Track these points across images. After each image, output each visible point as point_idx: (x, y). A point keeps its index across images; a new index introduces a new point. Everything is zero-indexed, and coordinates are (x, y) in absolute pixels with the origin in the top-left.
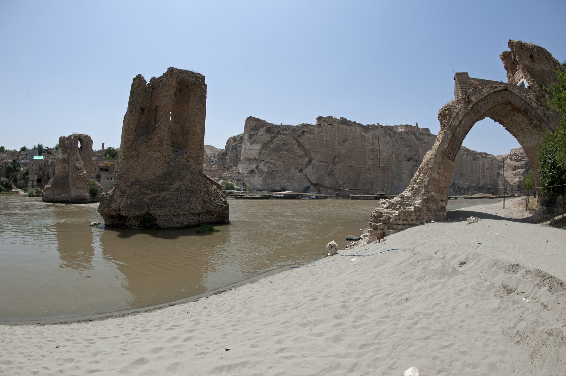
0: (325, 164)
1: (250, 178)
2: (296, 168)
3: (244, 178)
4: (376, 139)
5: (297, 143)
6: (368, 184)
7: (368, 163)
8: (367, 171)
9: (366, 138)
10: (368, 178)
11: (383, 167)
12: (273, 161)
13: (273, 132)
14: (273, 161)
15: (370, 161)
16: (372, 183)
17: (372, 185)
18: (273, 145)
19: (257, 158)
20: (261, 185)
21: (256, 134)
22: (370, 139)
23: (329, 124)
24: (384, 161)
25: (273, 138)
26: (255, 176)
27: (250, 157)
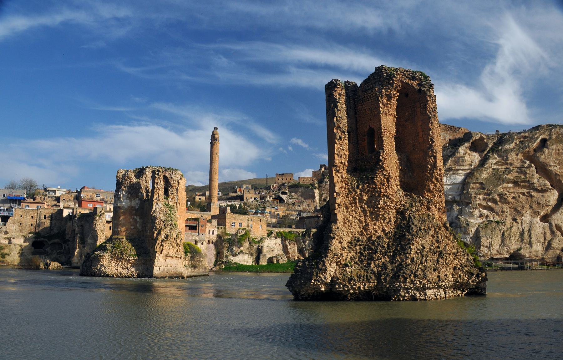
2: (535, 213)
5: (533, 165)
18: (486, 173)
19: (458, 199)
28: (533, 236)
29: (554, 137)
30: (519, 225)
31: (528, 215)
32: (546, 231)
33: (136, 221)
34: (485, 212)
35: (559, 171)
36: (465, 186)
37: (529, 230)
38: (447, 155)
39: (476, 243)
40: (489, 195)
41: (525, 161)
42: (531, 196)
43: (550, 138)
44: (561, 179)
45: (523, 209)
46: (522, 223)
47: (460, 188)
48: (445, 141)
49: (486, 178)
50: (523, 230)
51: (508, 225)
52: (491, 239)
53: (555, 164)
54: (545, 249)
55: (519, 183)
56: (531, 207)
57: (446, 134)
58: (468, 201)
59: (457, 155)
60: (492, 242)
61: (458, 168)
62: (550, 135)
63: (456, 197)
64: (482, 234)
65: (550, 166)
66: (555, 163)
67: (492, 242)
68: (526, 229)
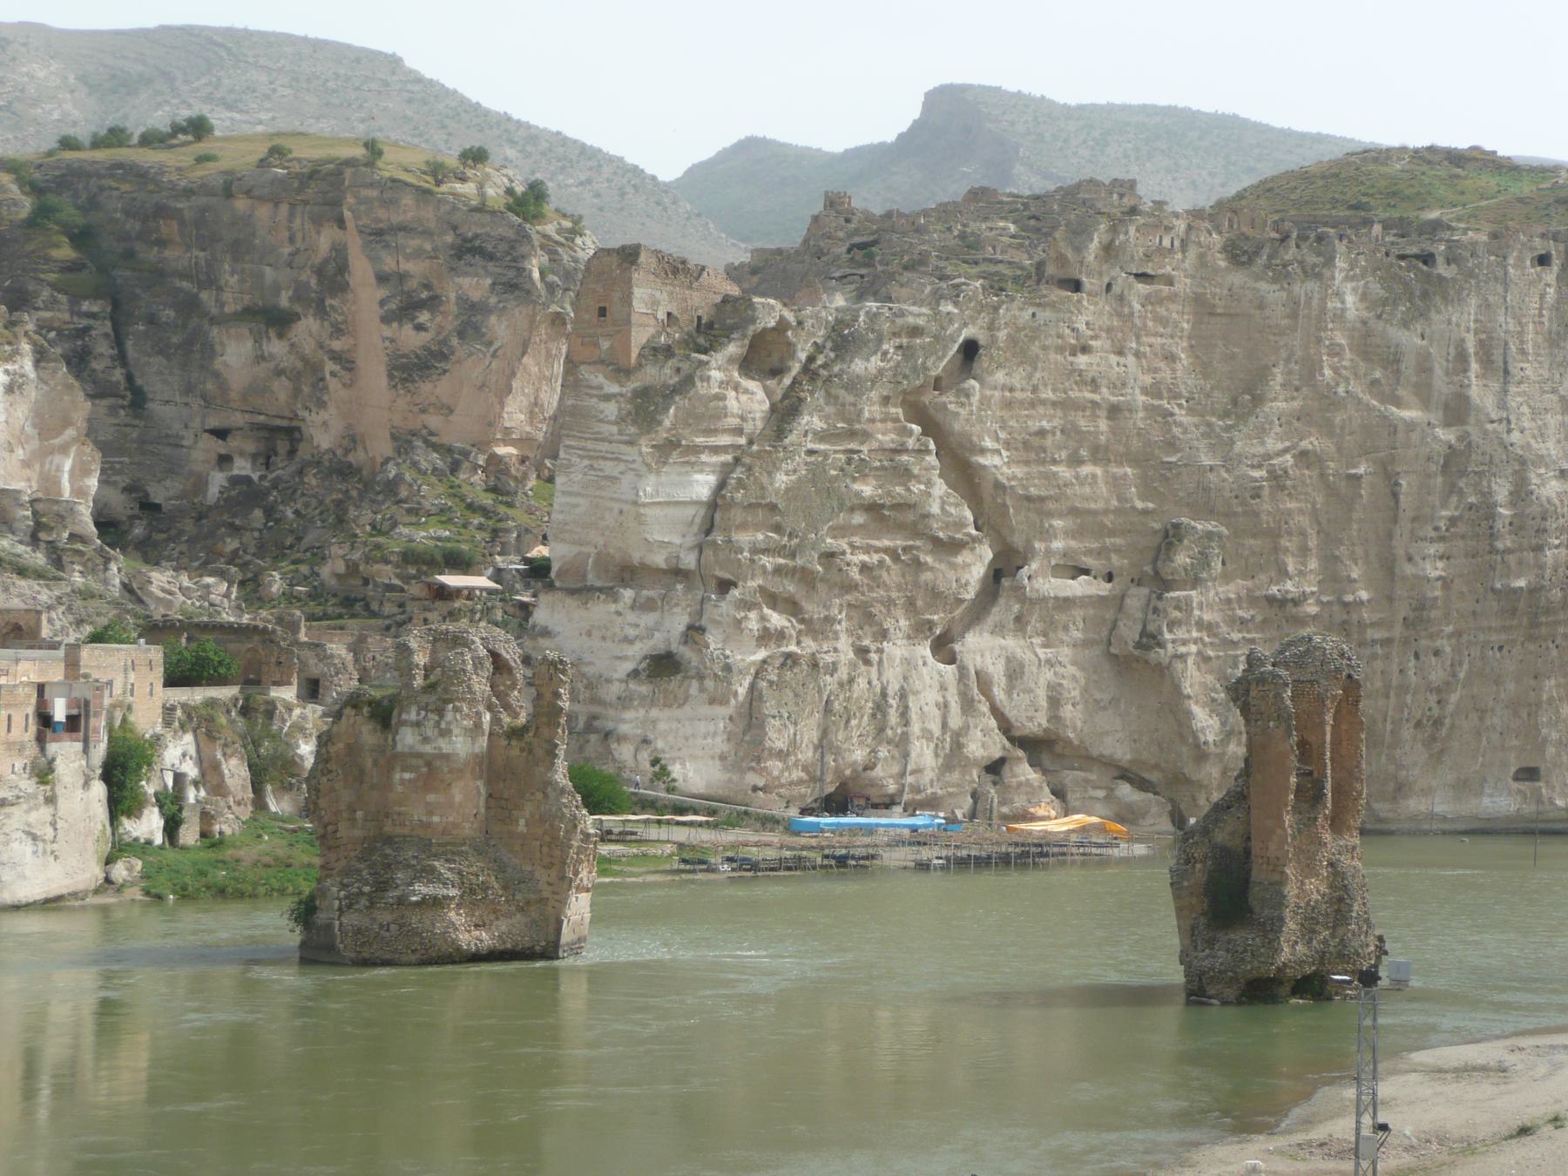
0: (1103, 588)
1: (654, 713)
2: (921, 629)
3: (596, 709)
4: (1487, 361)
6: (1407, 732)
7: (1409, 569)
8: (1398, 631)
9: (1408, 366)
10: (1403, 689)
11: (1534, 591)
12: (790, 587)
13: (774, 361)
14: (791, 588)
15: (1432, 550)
16: (1437, 723)
17: (1433, 739)
19: (689, 561)
20: (723, 758)
22: (1439, 372)
23: (1142, 277)
24: (1538, 549)
25: (784, 413)
26: (687, 698)
27: (636, 557)
28: (914, 715)
29: (1002, 335)
30: (874, 670)
31: (901, 635)
32: (949, 699)
33: (477, 788)
34: (777, 620)
35: (1005, 469)
36: (717, 516)
37: (903, 695)
38: (665, 386)
39: (747, 738)
40: (793, 556)
41: (909, 425)
42: (918, 565)
43: (994, 339)
44: (1009, 502)
45: (889, 610)
46: (880, 662)
47: (698, 520)
48: (652, 322)
49: (788, 490)
50: (884, 694)
51: (843, 673)
52: (796, 724)
53: (996, 446)
54: (940, 761)
55: (887, 513)
56: (910, 604)
57: (658, 294)
58: (726, 575)
60: (795, 734)
61: (700, 440)
62: (991, 327)
63: (682, 555)
64: (769, 707)
65: (983, 451)
66: (997, 439)
67: (795, 734)
68: (893, 688)
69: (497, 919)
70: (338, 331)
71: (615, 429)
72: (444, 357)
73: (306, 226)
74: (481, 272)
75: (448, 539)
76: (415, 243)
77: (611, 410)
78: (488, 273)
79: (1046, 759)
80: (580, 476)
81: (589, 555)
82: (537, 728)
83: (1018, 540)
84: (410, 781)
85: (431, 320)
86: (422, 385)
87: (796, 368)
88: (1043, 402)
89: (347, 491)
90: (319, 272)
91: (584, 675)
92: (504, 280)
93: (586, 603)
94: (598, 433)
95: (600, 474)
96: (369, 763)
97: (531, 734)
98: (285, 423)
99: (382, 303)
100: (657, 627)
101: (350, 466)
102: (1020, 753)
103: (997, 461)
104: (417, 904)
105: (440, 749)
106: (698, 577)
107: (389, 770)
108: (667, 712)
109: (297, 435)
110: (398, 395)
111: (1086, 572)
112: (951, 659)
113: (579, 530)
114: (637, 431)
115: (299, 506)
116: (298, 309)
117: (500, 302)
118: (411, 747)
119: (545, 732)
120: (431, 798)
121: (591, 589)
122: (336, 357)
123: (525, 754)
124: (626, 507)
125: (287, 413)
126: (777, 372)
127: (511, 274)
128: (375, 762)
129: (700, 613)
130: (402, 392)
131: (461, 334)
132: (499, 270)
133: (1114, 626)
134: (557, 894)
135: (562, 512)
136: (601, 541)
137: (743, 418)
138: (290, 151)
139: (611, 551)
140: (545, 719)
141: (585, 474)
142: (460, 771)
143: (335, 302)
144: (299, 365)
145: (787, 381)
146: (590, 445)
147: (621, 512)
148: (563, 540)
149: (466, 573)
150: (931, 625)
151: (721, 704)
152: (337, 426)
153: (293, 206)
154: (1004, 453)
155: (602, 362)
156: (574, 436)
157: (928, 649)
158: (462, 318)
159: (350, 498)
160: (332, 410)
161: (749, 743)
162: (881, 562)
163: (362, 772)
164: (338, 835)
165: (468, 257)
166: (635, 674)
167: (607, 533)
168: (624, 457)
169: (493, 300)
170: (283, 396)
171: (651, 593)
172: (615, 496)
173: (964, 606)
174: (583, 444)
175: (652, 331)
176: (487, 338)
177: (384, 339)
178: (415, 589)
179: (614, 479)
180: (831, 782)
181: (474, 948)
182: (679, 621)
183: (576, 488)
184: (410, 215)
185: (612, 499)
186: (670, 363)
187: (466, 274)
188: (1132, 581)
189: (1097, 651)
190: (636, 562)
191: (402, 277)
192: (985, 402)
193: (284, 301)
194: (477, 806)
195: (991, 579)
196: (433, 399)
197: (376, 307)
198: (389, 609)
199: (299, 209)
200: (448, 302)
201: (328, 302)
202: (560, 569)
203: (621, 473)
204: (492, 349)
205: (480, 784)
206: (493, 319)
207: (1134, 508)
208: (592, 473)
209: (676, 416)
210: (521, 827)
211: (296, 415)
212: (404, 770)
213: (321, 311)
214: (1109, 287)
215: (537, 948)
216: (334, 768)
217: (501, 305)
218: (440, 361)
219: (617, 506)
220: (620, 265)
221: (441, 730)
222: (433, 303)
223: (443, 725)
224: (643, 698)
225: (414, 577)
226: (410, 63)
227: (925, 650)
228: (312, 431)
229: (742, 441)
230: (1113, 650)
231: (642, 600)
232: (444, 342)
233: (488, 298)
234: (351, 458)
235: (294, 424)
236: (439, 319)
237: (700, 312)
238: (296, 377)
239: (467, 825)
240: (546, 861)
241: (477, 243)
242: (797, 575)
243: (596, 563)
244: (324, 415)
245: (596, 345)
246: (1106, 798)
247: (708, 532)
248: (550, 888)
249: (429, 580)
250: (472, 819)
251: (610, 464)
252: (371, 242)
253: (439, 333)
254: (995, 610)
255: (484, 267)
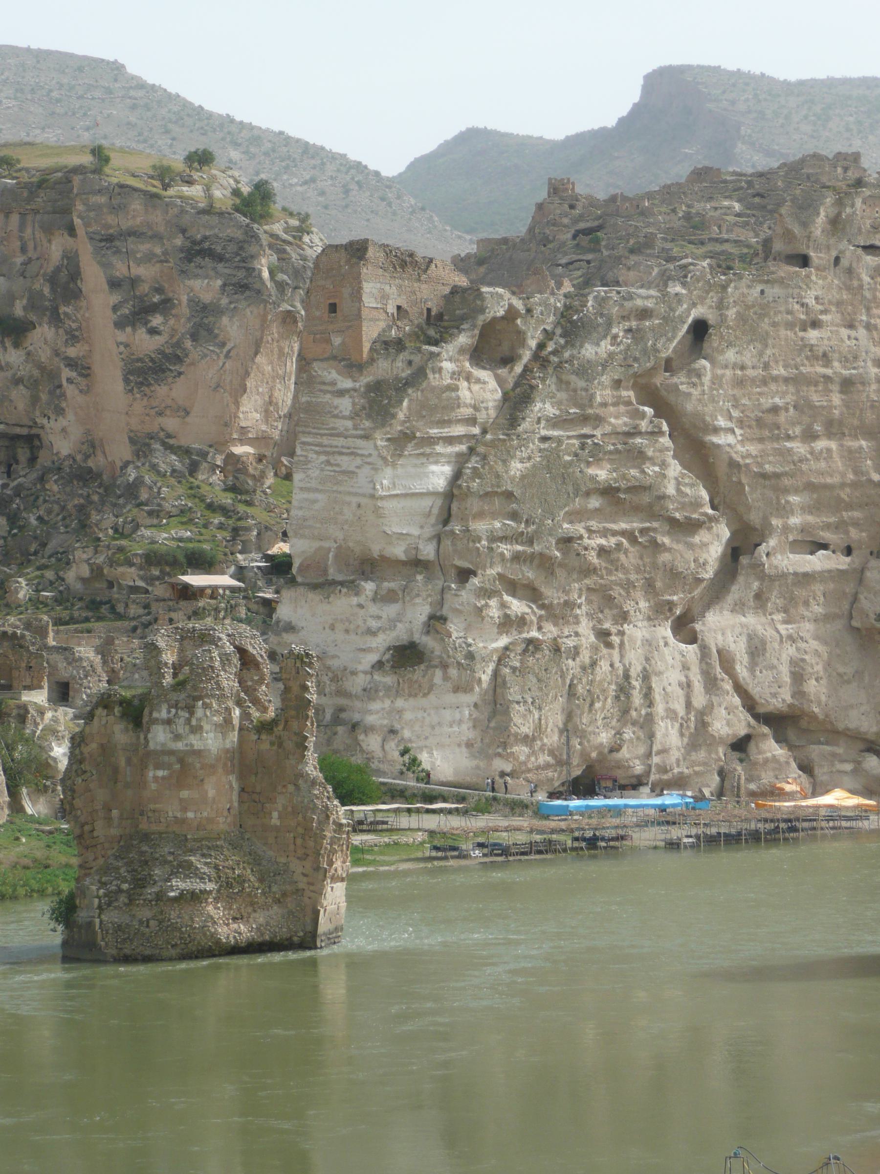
0: (842, 562)
1: (400, 703)
2: (661, 609)
3: (342, 701)
12: (529, 574)
13: (505, 348)
14: (530, 575)
19: (428, 551)
20: (469, 745)
21: (409, 383)
27: (376, 549)
28: (657, 696)
29: (731, 313)
30: (616, 653)
31: (641, 617)
32: (692, 678)
34: (517, 606)
35: (739, 448)
36: (454, 507)
37: (646, 677)
38: (397, 379)
39: (492, 724)
40: (530, 542)
41: (641, 408)
42: (656, 546)
43: (723, 318)
44: (744, 480)
45: (628, 593)
46: (622, 645)
47: (435, 511)
48: (383, 316)
49: (523, 477)
50: (627, 676)
52: (540, 709)
53: (729, 425)
54: (686, 740)
55: (622, 496)
56: (650, 587)
57: (387, 287)
58: (465, 564)
59: (433, 379)
60: (540, 719)
61: (434, 431)
62: (721, 306)
63: (421, 547)
64: (513, 693)
65: (716, 430)
66: (730, 418)
67: (540, 719)
69: (255, 911)
70: (73, 338)
71: (349, 424)
72: (178, 360)
73: (37, 236)
74: (212, 273)
75: (189, 540)
76: (144, 247)
77: (345, 405)
78: (218, 275)
79: (791, 734)
80: (318, 472)
81: (329, 549)
82: (286, 722)
83: (754, 518)
84: (163, 778)
85: (164, 324)
86: (158, 388)
87: (526, 356)
88: (775, 379)
89: (89, 496)
90: (52, 280)
91: (329, 668)
92: (234, 280)
93: (328, 597)
94: (333, 428)
95: (337, 469)
96: (122, 763)
97: (281, 727)
98: (24, 431)
99: (115, 308)
100: (399, 618)
101: (90, 470)
102: (766, 730)
103: (730, 439)
104: (175, 899)
105: (192, 745)
106: (439, 568)
107: (143, 767)
108: (412, 702)
109: (37, 443)
110: (135, 399)
111: (824, 546)
112: (692, 639)
113: (318, 525)
114: (372, 425)
115: (41, 513)
116: (33, 317)
117: (231, 303)
118: (163, 745)
119: (295, 725)
120: (185, 794)
121: (334, 583)
122: (72, 363)
123: (275, 748)
124: (364, 501)
125: (26, 421)
126: (508, 361)
127: (241, 274)
128: (129, 761)
129: (441, 603)
130: (138, 396)
131: (194, 337)
132: (227, 271)
133: (855, 599)
134: (312, 884)
135: (301, 508)
136: (340, 535)
137: (476, 408)
138: (18, 161)
139: (351, 544)
140: (293, 713)
141: (322, 470)
142: (213, 766)
143: (69, 310)
144: (36, 373)
145: (518, 369)
146: (325, 441)
147: (359, 506)
148: (303, 536)
149: (208, 573)
150: (671, 605)
151: (465, 691)
152: (76, 433)
153: (23, 215)
154: (738, 431)
155: (334, 358)
156: (309, 433)
157: (669, 630)
158: (195, 320)
159: (92, 503)
160: (70, 416)
161: (495, 729)
162: (619, 545)
163: (116, 770)
164: (95, 834)
165: (198, 259)
166: (379, 665)
167: (346, 527)
168: (359, 452)
169: (224, 301)
170: (21, 406)
171: (392, 585)
172: (351, 490)
173: (705, 583)
174: (319, 440)
175: (382, 324)
176: (221, 338)
177: (118, 344)
178: (159, 590)
179: (350, 474)
180: (578, 765)
181: (233, 941)
182: (420, 612)
183: (314, 484)
184: (139, 220)
185: (350, 493)
186: (401, 356)
187: (196, 276)
188: (871, 553)
189: (839, 624)
190: (376, 555)
191: (134, 282)
192: (717, 381)
193: (18, 311)
194: (231, 801)
195: (729, 558)
196: (169, 402)
197: (109, 312)
198: (134, 610)
199: (29, 218)
200: (180, 304)
201: (63, 309)
202: (301, 565)
203: (358, 467)
204: (225, 350)
205: (233, 778)
206: (225, 320)
207: (870, 481)
208: (328, 468)
209: (409, 408)
210: (275, 820)
211: (36, 423)
212: (157, 767)
213: (56, 319)
214: (837, 260)
215: (295, 939)
216: (88, 768)
217: (232, 306)
218: (175, 364)
219: (354, 500)
220: (348, 262)
221: (191, 727)
222: (165, 306)
223: (194, 722)
224: (388, 689)
225: (158, 578)
226: (132, 69)
227: (665, 631)
228: (52, 438)
229: (476, 430)
230: (855, 623)
231: (384, 592)
232: (178, 345)
233: (220, 299)
234: (90, 463)
235: (34, 431)
236: (172, 322)
237: (430, 304)
238: (33, 385)
239: (221, 820)
240: (300, 852)
241: (206, 245)
242: (536, 562)
243: (336, 556)
244: (62, 422)
245: (328, 341)
246: (855, 771)
247: (446, 522)
248: (305, 879)
249: (173, 580)
250: (226, 813)
251: (345, 458)
252: (102, 248)
253: (172, 336)
254: (734, 588)
255: (214, 269)
